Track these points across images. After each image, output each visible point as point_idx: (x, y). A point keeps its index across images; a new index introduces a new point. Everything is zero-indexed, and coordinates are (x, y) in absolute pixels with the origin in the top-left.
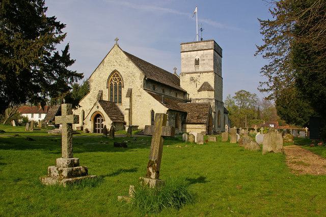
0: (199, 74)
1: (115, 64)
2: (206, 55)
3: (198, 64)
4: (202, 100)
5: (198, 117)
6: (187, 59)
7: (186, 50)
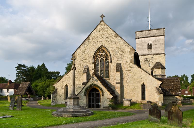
0: (152, 56)
1: (102, 40)
2: (158, 40)
6: (141, 44)
7: (140, 37)
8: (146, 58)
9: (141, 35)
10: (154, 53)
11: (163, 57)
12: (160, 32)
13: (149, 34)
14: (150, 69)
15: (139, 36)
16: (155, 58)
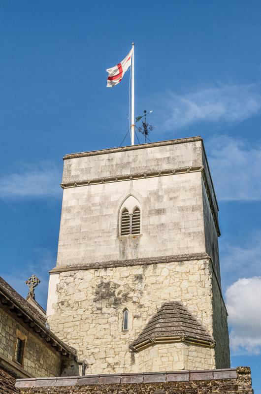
0: (138, 270)
2: (168, 191)
3: (136, 231)
6: (87, 209)
7: (81, 179)
8: (109, 284)
9: (88, 170)
10: (149, 255)
11: (196, 277)
13: (129, 163)
14: (126, 347)
15: (77, 176)
16: (153, 279)
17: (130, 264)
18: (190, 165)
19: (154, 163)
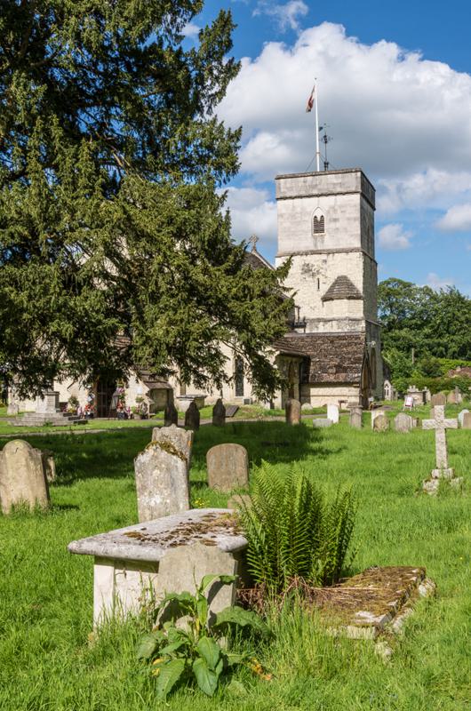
0: (324, 257)
2: (341, 206)
3: (323, 231)
4: (334, 323)
5: (340, 368)
6: (293, 216)
7: (288, 195)
9: (291, 189)
11: (355, 262)
12: (346, 180)
13: (316, 185)
14: (320, 298)
15: (285, 192)
16: (333, 263)
17: (319, 253)
18: (353, 189)
19: (332, 186)
